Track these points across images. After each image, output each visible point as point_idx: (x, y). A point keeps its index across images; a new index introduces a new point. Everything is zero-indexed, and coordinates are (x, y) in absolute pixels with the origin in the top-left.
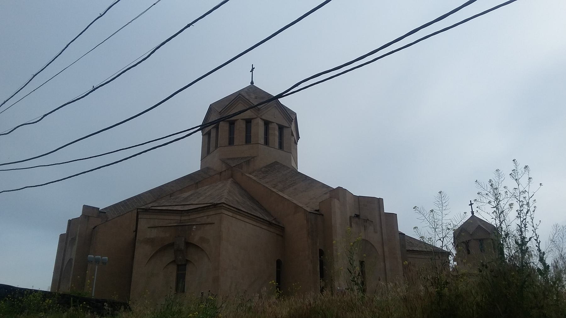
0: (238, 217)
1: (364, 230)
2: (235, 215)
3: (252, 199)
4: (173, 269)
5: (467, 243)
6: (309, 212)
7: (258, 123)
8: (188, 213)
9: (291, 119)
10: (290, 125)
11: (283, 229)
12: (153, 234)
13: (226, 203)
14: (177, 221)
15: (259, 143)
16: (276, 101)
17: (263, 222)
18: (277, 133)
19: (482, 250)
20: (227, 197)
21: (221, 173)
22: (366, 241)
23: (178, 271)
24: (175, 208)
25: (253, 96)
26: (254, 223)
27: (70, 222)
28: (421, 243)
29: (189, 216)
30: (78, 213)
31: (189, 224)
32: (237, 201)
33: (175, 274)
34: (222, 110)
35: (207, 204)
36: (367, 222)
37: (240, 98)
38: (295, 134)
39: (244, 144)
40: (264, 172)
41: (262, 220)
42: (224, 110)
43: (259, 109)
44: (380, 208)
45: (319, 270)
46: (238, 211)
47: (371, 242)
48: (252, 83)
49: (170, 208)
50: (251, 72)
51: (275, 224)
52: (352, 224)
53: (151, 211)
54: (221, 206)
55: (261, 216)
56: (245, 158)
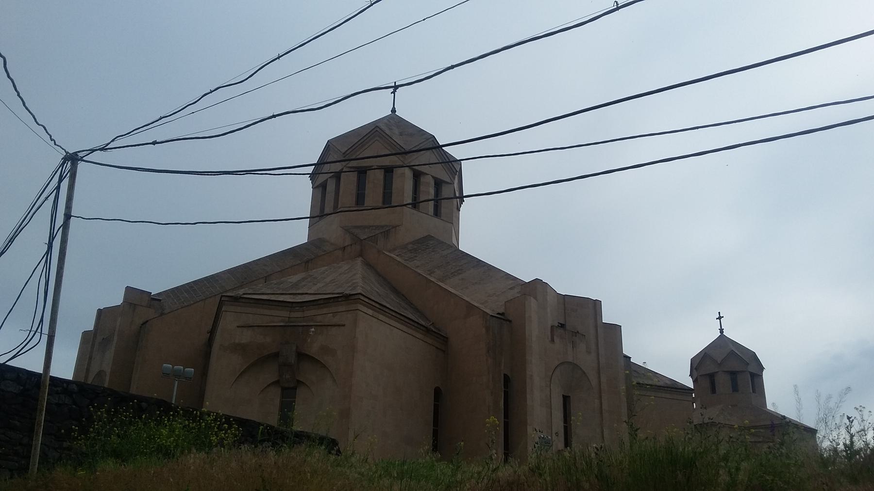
0: (381, 317)
2: (376, 315)
3: (396, 291)
4: (275, 395)
5: (711, 377)
6: (491, 315)
7: (404, 173)
8: (301, 307)
9: (455, 171)
10: (452, 178)
11: (445, 340)
12: (246, 337)
13: (364, 294)
14: (283, 318)
16: (433, 141)
19: (735, 388)
20: (363, 285)
21: (344, 247)
22: (575, 366)
24: (281, 298)
25: (397, 131)
27: (100, 312)
30: (117, 299)
31: (305, 324)
32: (377, 292)
33: (277, 402)
34: (347, 151)
35: (333, 294)
36: (576, 336)
39: (380, 205)
40: (411, 250)
41: (416, 325)
42: (351, 150)
44: (596, 315)
45: (503, 407)
46: (382, 309)
48: (394, 111)
49: (273, 298)
50: (393, 94)
52: (555, 337)
53: (244, 300)
54: (357, 299)
55: (413, 318)
56: (382, 227)
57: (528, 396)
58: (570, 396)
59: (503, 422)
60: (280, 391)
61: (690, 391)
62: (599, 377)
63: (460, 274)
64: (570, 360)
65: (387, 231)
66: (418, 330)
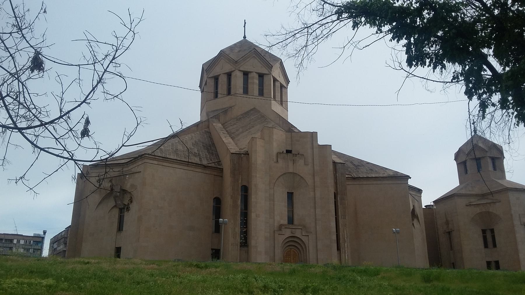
1: (292, 164)
4: (116, 212)
6: (232, 153)
7: (236, 75)
9: (271, 66)
11: (222, 170)
18: (256, 81)
22: (294, 174)
23: (121, 214)
25: (237, 50)
26: (186, 168)
28: (383, 169)
33: (117, 216)
36: (296, 156)
37: (221, 54)
38: (281, 80)
41: (195, 165)
42: (209, 67)
43: (236, 62)
44: (313, 141)
45: (240, 204)
47: (299, 174)
48: (245, 37)
53: (100, 166)
56: (225, 108)
57: (253, 196)
58: (293, 192)
59: (287, 210)
60: (118, 211)
61: (405, 178)
62: (314, 179)
63: (251, 129)
64: (291, 170)
65: (226, 110)
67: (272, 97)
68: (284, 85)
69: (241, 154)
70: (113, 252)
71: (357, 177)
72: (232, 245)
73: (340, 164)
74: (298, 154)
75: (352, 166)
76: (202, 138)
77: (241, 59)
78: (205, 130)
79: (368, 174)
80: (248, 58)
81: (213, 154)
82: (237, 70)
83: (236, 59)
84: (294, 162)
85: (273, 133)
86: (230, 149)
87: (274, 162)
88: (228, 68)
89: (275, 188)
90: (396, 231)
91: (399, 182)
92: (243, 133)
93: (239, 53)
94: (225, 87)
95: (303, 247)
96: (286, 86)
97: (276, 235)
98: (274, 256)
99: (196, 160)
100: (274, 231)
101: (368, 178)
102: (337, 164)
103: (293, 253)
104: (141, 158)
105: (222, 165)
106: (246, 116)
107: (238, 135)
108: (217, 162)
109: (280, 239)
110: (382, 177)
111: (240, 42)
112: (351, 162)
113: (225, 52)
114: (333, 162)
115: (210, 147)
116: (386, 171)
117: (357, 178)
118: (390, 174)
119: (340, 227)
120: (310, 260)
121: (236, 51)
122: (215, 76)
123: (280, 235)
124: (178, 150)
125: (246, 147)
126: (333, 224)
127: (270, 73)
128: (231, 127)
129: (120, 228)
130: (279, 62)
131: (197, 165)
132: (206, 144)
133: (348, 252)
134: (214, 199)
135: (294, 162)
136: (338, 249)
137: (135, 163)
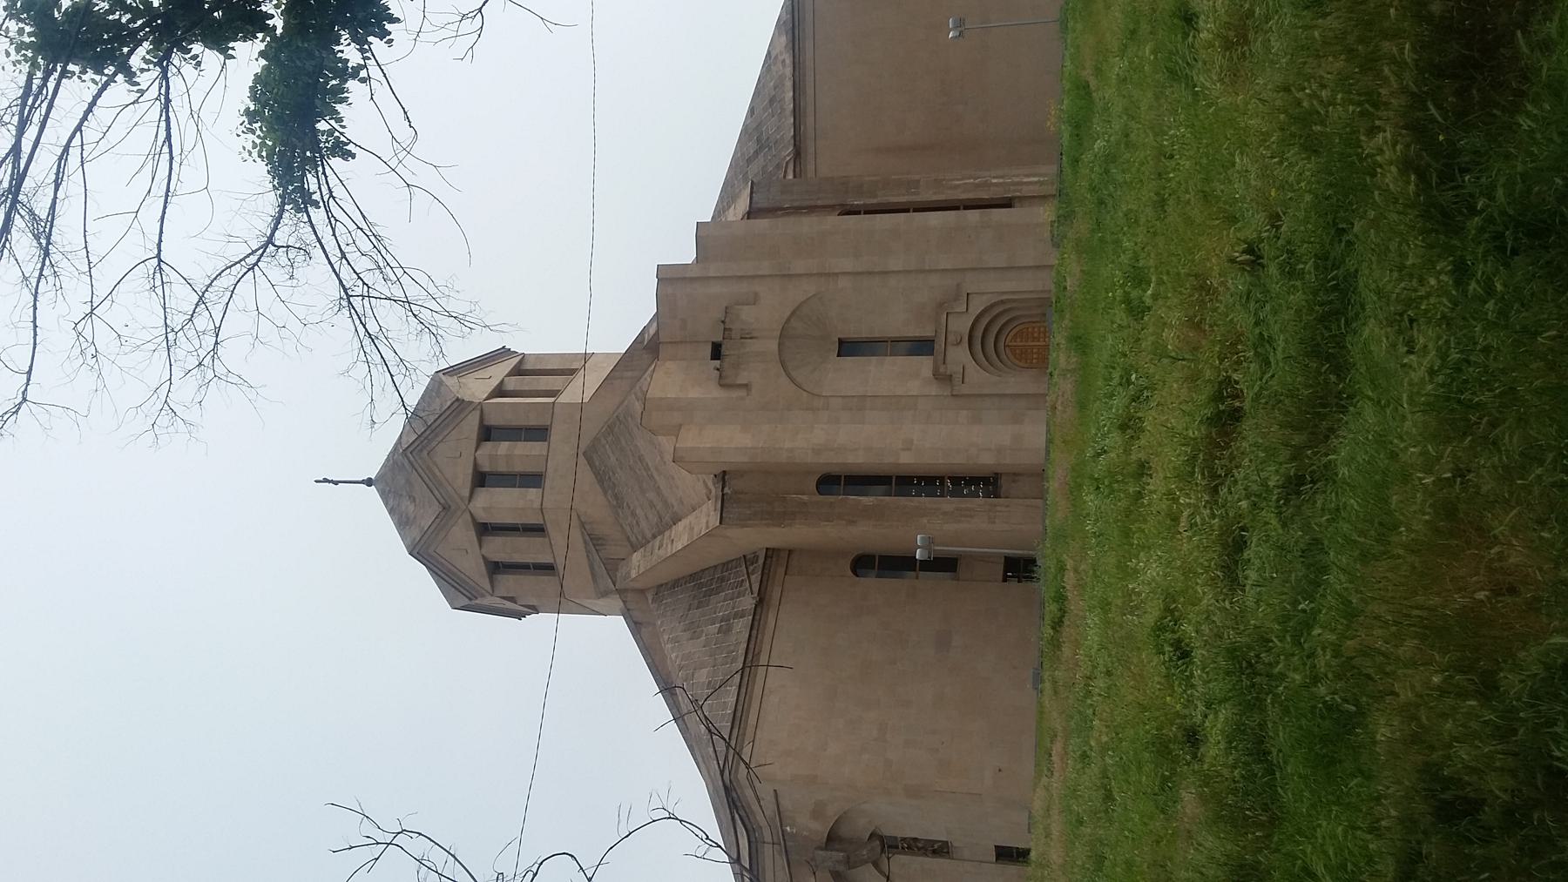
1: (754, 340)
6: (721, 523)
7: (484, 508)
9: (456, 404)
11: (771, 553)
14: (775, 853)
15: (537, 505)
17: (758, 631)
18: (504, 447)
22: (784, 336)
29: (761, 828)
36: (730, 330)
37: (421, 552)
38: (499, 372)
39: (547, 540)
41: (754, 632)
43: (444, 508)
45: (871, 499)
48: (369, 482)
51: (761, 581)
52: (738, 382)
56: (585, 542)
59: (892, 358)
63: (647, 464)
65: (591, 539)
66: (762, 622)
67: (551, 400)
68: (515, 363)
69: (723, 495)
70: (1012, 869)
71: (795, 145)
72: (994, 523)
73: (754, 195)
74: (723, 322)
75: (761, 160)
76: (674, 610)
77: (436, 492)
78: (650, 601)
79: (783, 109)
80: (434, 475)
81: (722, 579)
82: (471, 506)
83: (437, 508)
84: (747, 336)
85: (661, 399)
86: (707, 527)
87: (748, 395)
88: (462, 533)
89: (824, 394)
90: (955, 28)
91: (809, 17)
92: (659, 487)
93: (417, 501)
94: (522, 541)
95: (1001, 309)
96: (521, 357)
97: (965, 389)
98: (1027, 396)
99: (741, 627)
100: (952, 395)
101: (797, 112)
102: (753, 205)
103: (1018, 340)
104: (735, 790)
105: (755, 553)
106: (609, 478)
107: (665, 502)
108: (747, 568)
109: (977, 378)
110: (794, 67)
111: (384, 495)
112: (749, 161)
113: (414, 539)
114: (748, 218)
115: (700, 586)
116: (776, 57)
117: (797, 143)
118: (784, 45)
119: (944, 198)
120: (1041, 289)
121: (411, 508)
122: (488, 572)
123: (966, 380)
124: (710, 682)
125: (702, 481)
126: (934, 218)
127: (479, 407)
128: (643, 524)
129: (940, 850)
130: (446, 379)
131: (755, 626)
132: (694, 598)
133: (1018, 176)
134: (857, 576)
135: (747, 336)
136: (1007, 204)
137: (750, 807)
